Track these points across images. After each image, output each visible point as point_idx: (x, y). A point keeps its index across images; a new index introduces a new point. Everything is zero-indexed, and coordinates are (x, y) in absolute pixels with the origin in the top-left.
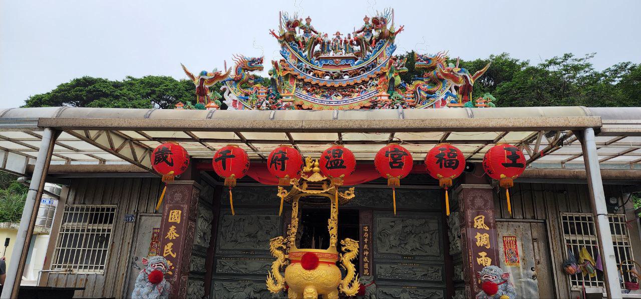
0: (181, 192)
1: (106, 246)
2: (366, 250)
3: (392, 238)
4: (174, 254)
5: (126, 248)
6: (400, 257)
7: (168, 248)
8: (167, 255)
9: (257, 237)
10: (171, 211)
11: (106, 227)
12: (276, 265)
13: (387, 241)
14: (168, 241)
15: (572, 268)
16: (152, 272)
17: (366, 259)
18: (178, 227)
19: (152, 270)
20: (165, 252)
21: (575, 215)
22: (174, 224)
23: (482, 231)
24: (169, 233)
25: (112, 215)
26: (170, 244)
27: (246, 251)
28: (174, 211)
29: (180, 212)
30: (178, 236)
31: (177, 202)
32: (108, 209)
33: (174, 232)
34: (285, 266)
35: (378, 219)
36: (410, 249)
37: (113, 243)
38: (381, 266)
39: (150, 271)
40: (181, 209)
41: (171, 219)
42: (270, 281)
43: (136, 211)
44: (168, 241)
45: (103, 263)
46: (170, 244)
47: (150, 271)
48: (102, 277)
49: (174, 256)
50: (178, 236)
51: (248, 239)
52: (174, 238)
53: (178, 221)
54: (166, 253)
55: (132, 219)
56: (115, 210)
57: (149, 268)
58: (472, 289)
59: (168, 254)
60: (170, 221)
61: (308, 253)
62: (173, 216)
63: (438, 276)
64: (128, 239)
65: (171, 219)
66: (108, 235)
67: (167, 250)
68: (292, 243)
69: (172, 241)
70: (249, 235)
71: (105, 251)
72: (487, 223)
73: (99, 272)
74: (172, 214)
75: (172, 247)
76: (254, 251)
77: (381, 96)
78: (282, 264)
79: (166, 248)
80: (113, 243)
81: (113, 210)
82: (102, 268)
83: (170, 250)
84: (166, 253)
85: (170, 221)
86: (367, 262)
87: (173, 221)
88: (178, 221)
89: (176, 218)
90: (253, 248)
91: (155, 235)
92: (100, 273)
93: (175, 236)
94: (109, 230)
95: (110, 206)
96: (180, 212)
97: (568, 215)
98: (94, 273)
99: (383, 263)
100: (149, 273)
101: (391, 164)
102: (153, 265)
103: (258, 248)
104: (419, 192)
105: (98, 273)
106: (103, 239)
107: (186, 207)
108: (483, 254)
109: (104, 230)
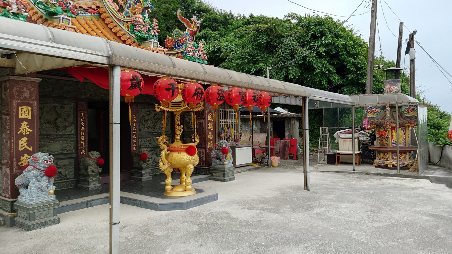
0: (29, 90)
3: (149, 122)
4: (30, 148)
7: (23, 142)
8: (23, 149)
9: (55, 123)
10: (20, 108)
12: (163, 153)
13: (146, 124)
14: (22, 136)
15: (223, 135)
16: (46, 168)
17: (134, 136)
18: (30, 123)
19: (46, 166)
20: (20, 146)
21: (224, 110)
22: (26, 120)
23: (211, 122)
26: (24, 139)
27: (45, 135)
29: (30, 108)
30: (31, 131)
31: (25, 99)
33: (26, 127)
34: (168, 154)
35: (140, 109)
36: (158, 128)
38: (142, 139)
41: (22, 115)
42: (161, 164)
44: (22, 136)
46: (24, 139)
47: (43, 167)
50: (31, 131)
51: (48, 126)
52: (28, 133)
53: (30, 117)
54: (22, 147)
57: (42, 165)
58: (206, 151)
59: (24, 148)
60: (20, 117)
61: (190, 146)
62: (23, 112)
65: (22, 115)
67: (22, 145)
68: (178, 140)
69: (26, 136)
70: (49, 122)
72: (212, 117)
74: (22, 111)
75: (27, 141)
76: (53, 135)
77: (139, 17)
78: (167, 153)
83: (25, 144)
84: (22, 147)
85: (20, 117)
87: (23, 117)
88: (30, 117)
89: (27, 114)
90: (53, 133)
93: (28, 131)
96: (30, 108)
97: (222, 109)
99: (144, 138)
100: (42, 169)
101: (241, 99)
102: (45, 162)
103: (58, 133)
107: (35, 104)
108: (210, 133)
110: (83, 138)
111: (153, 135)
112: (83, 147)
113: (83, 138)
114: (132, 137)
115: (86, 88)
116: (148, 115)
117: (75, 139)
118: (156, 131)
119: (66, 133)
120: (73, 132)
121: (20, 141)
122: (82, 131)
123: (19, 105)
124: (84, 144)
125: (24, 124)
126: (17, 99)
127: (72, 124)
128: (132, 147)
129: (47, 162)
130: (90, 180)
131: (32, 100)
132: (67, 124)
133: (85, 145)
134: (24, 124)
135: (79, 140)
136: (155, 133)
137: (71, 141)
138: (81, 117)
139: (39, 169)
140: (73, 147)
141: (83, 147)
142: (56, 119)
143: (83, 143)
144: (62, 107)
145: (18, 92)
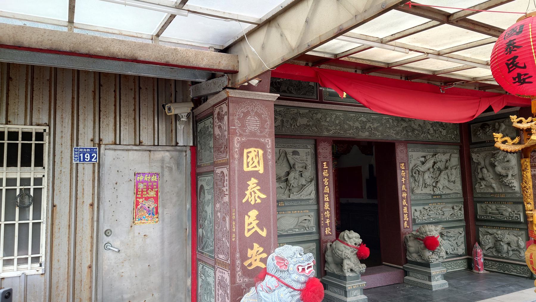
0: (259, 115)
1: (37, 214)
2: (404, 191)
3: (426, 176)
4: (262, 230)
5: (85, 213)
6: (430, 197)
7: (251, 220)
9: (287, 180)
10: (246, 151)
11: (31, 172)
14: (248, 207)
16: (302, 283)
17: (404, 203)
20: (247, 227)
22: (255, 174)
24: (247, 193)
25: (40, 149)
26: (253, 213)
28: (252, 149)
29: (261, 152)
31: (253, 134)
32: (27, 136)
33: (255, 189)
36: (441, 187)
37: (54, 206)
39: (298, 281)
40: (263, 147)
41: (248, 166)
43: (97, 141)
44: (248, 207)
45: (36, 248)
46: (253, 213)
47: (298, 281)
48: (42, 278)
49: (264, 234)
52: (259, 201)
53: (261, 169)
54: (249, 230)
55: (91, 157)
56: (46, 138)
57: (295, 276)
59: (253, 231)
63: (461, 215)
64: (87, 198)
65: (248, 166)
66: (38, 191)
67: (249, 225)
69: (256, 206)
71: (36, 226)
73: (32, 269)
74: (248, 157)
75: (258, 217)
79: (247, 220)
80: (54, 206)
81: (40, 136)
82: (35, 260)
84: (249, 230)
85: (246, 169)
86: (405, 206)
87: (250, 169)
88: (261, 169)
89: (256, 163)
91: (141, 186)
92: (34, 272)
93: (259, 197)
94: (38, 181)
95: (34, 129)
96: (261, 152)
98: (19, 273)
102: (300, 268)
103: (292, 197)
104: (302, 111)
105: (28, 272)
106: (25, 200)
107: (269, 142)
109: (25, 181)
110: (327, 206)
111: (433, 199)
112: (328, 221)
113: (327, 206)
114: (400, 203)
115: (328, 120)
116: (423, 163)
117: (315, 207)
118: (437, 192)
119: (302, 197)
120: (313, 196)
121: (246, 217)
122: (326, 193)
123: (244, 145)
124: (328, 216)
125: (253, 182)
126: (241, 135)
127: (311, 181)
128: (402, 222)
129: (303, 269)
130: (349, 286)
131: (265, 137)
132: (304, 183)
133: (330, 218)
134: (253, 182)
135: (321, 210)
136: (436, 195)
137: (310, 211)
138: (323, 170)
139: (288, 286)
140: (312, 223)
141: (328, 221)
142: (288, 173)
143: (327, 214)
144: (295, 153)
145: (242, 120)
